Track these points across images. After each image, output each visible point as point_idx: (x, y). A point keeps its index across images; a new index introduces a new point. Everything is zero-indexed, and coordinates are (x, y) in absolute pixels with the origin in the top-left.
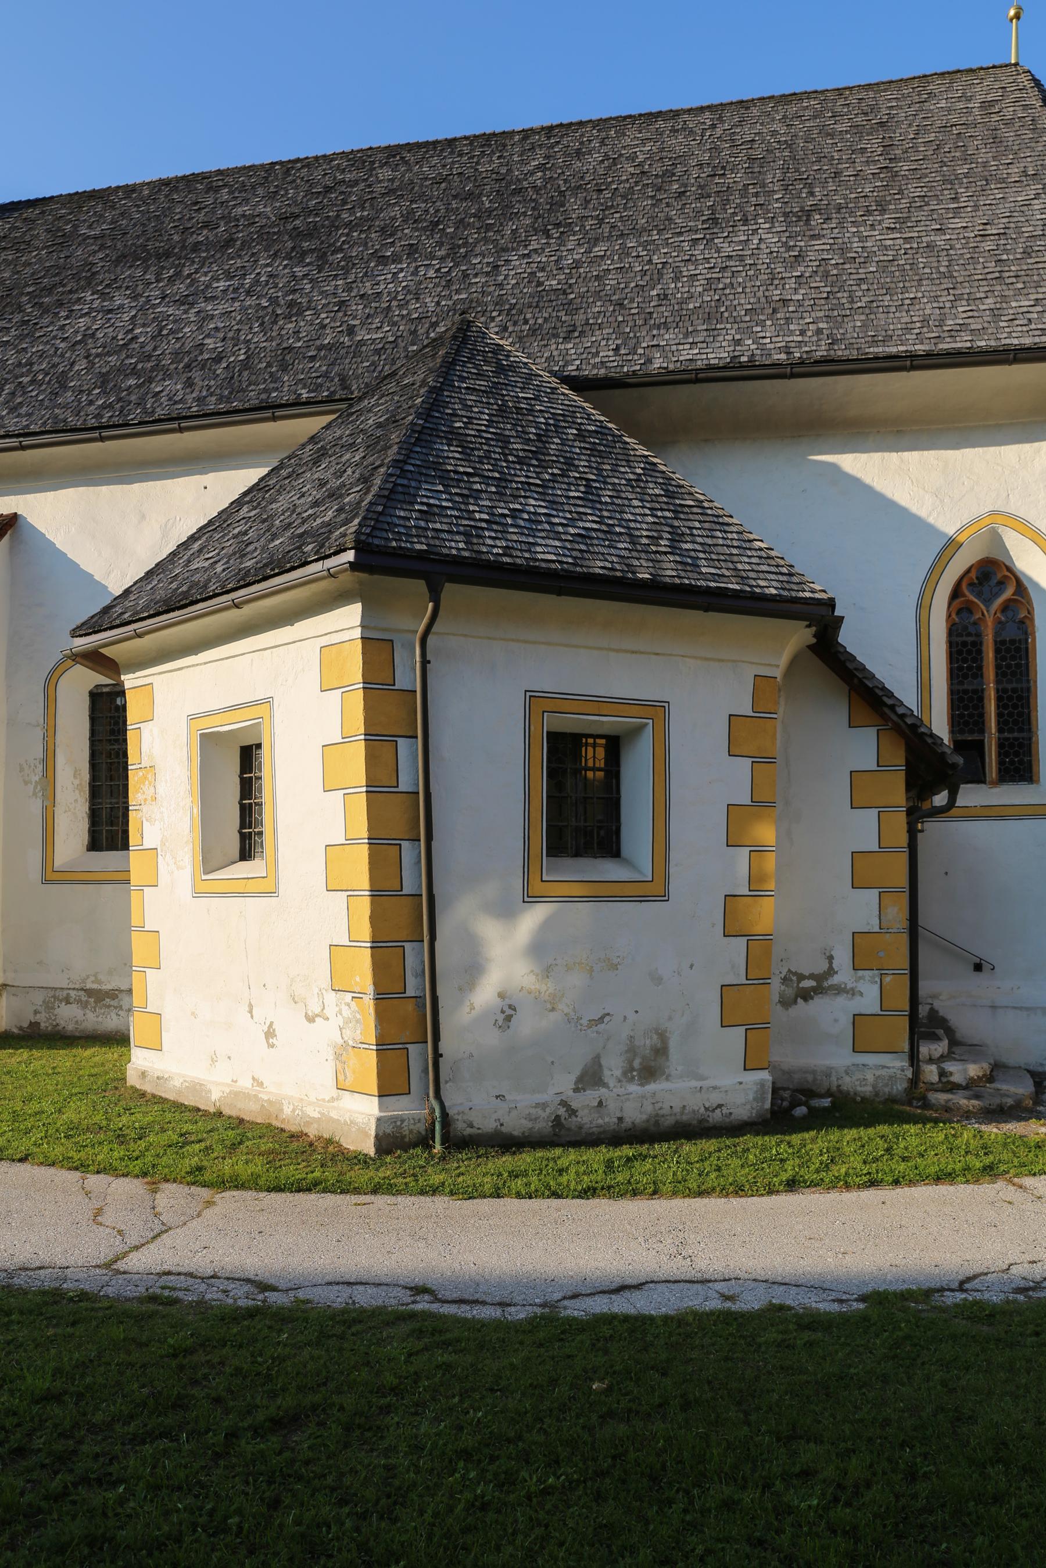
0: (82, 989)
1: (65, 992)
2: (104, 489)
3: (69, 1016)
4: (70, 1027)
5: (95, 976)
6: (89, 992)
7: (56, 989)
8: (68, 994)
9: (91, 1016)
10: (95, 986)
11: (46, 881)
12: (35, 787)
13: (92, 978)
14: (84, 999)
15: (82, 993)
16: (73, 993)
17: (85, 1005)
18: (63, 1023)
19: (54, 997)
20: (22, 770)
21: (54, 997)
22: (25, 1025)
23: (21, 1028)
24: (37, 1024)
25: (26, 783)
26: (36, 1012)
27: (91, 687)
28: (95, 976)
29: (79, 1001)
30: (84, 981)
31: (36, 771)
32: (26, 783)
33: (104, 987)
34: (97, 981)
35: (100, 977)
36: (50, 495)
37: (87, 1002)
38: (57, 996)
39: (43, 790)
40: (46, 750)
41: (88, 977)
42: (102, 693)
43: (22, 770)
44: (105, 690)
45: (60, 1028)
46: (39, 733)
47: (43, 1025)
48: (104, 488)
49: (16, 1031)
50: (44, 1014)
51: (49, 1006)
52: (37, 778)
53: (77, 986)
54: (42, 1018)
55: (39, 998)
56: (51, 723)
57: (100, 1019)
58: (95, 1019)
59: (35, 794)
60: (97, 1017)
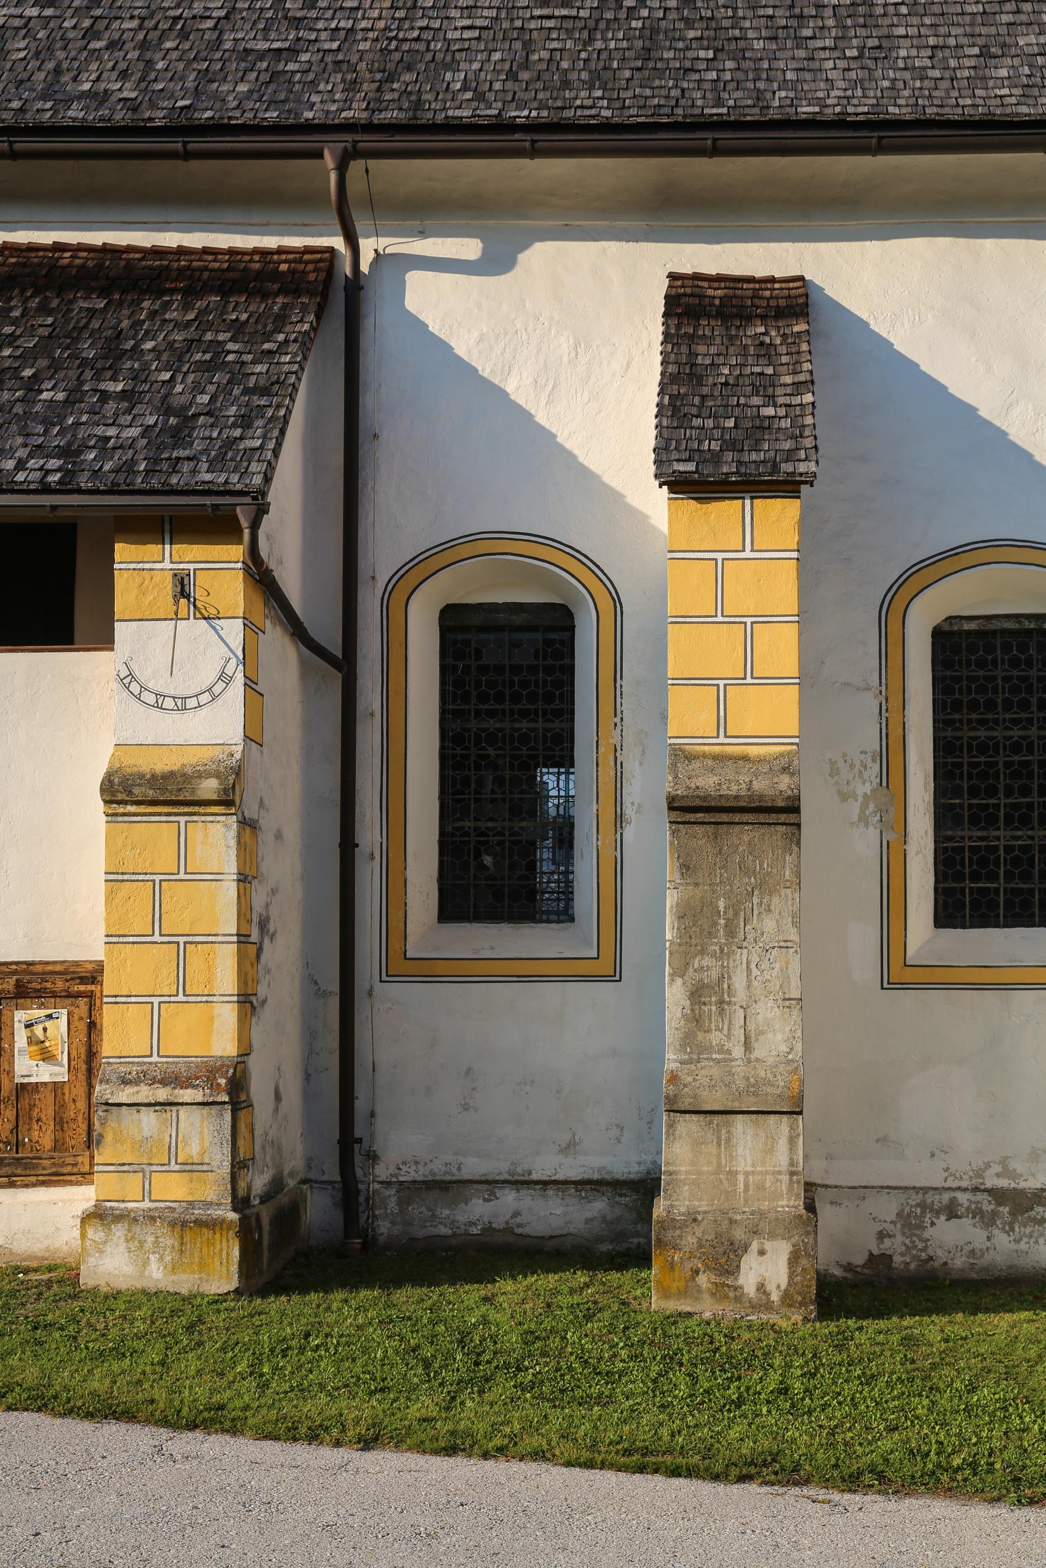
0: (976, 1190)
1: (946, 1197)
2: (989, 244)
3: (954, 1241)
4: (959, 1262)
5: (1003, 1162)
6: (999, 1195)
7: (925, 1190)
8: (953, 1201)
9: (1003, 1241)
10: (1004, 1183)
11: (889, 983)
12: (864, 806)
13: (997, 1168)
14: (988, 1207)
15: (984, 1197)
16: (963, 1198)
17: (988, 1220)
18: (942, 1256)
19: (923, 1205)
20: (834, 771)
21: (923, 1205)
22: (859, 1260)
23: (849, 1268)
24: (886, 1258)
25: (844, 797)
26: (882, 1236)
27: (938, 619)
28: (1003, 1162)
29: (977, 1213)
30: (979, 1174)
31: (866, 775)
32: (844, 797)
33: (1023, 1185)
34: (1013, 1175)
35: (1013, 1165)
36: (873, 247)
37: (994, 1214)
38: (925, 1205)
39: (882, 811)
40: (885, 736)
41: (988, 1165)
42: (960, 633)
43: (834, 771)
44: (967, 626)
45: (936, 1264)
46: (871, 703)
47: (897, 1259)
48: (989, 243)
49: (838, 1272)
50: (899, 1238)
51: (911, 1223)
52: (867, 788)
53: (964, 1184)
54: (896, 1246)
55: (887, 1209)
56: (895, 684)
57: (1023, 1246)
58: (1013, 1246)
59: (863, 819)
60: (1017, 1241)
